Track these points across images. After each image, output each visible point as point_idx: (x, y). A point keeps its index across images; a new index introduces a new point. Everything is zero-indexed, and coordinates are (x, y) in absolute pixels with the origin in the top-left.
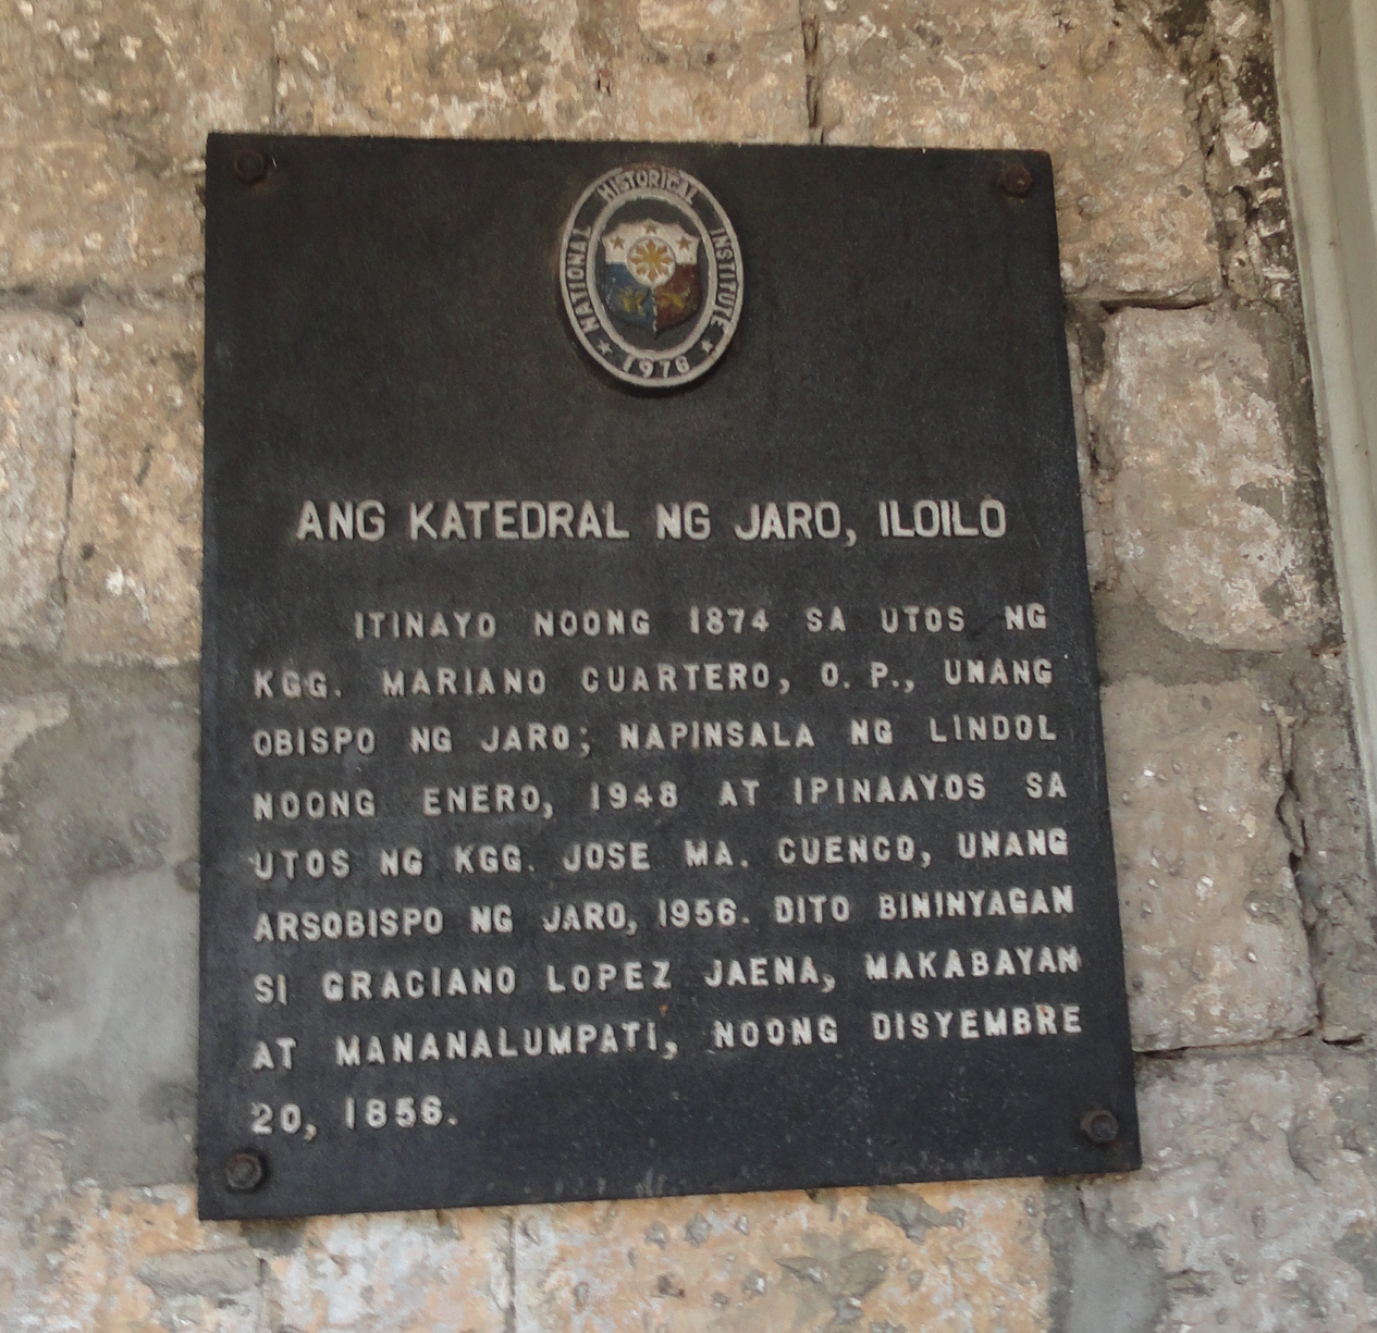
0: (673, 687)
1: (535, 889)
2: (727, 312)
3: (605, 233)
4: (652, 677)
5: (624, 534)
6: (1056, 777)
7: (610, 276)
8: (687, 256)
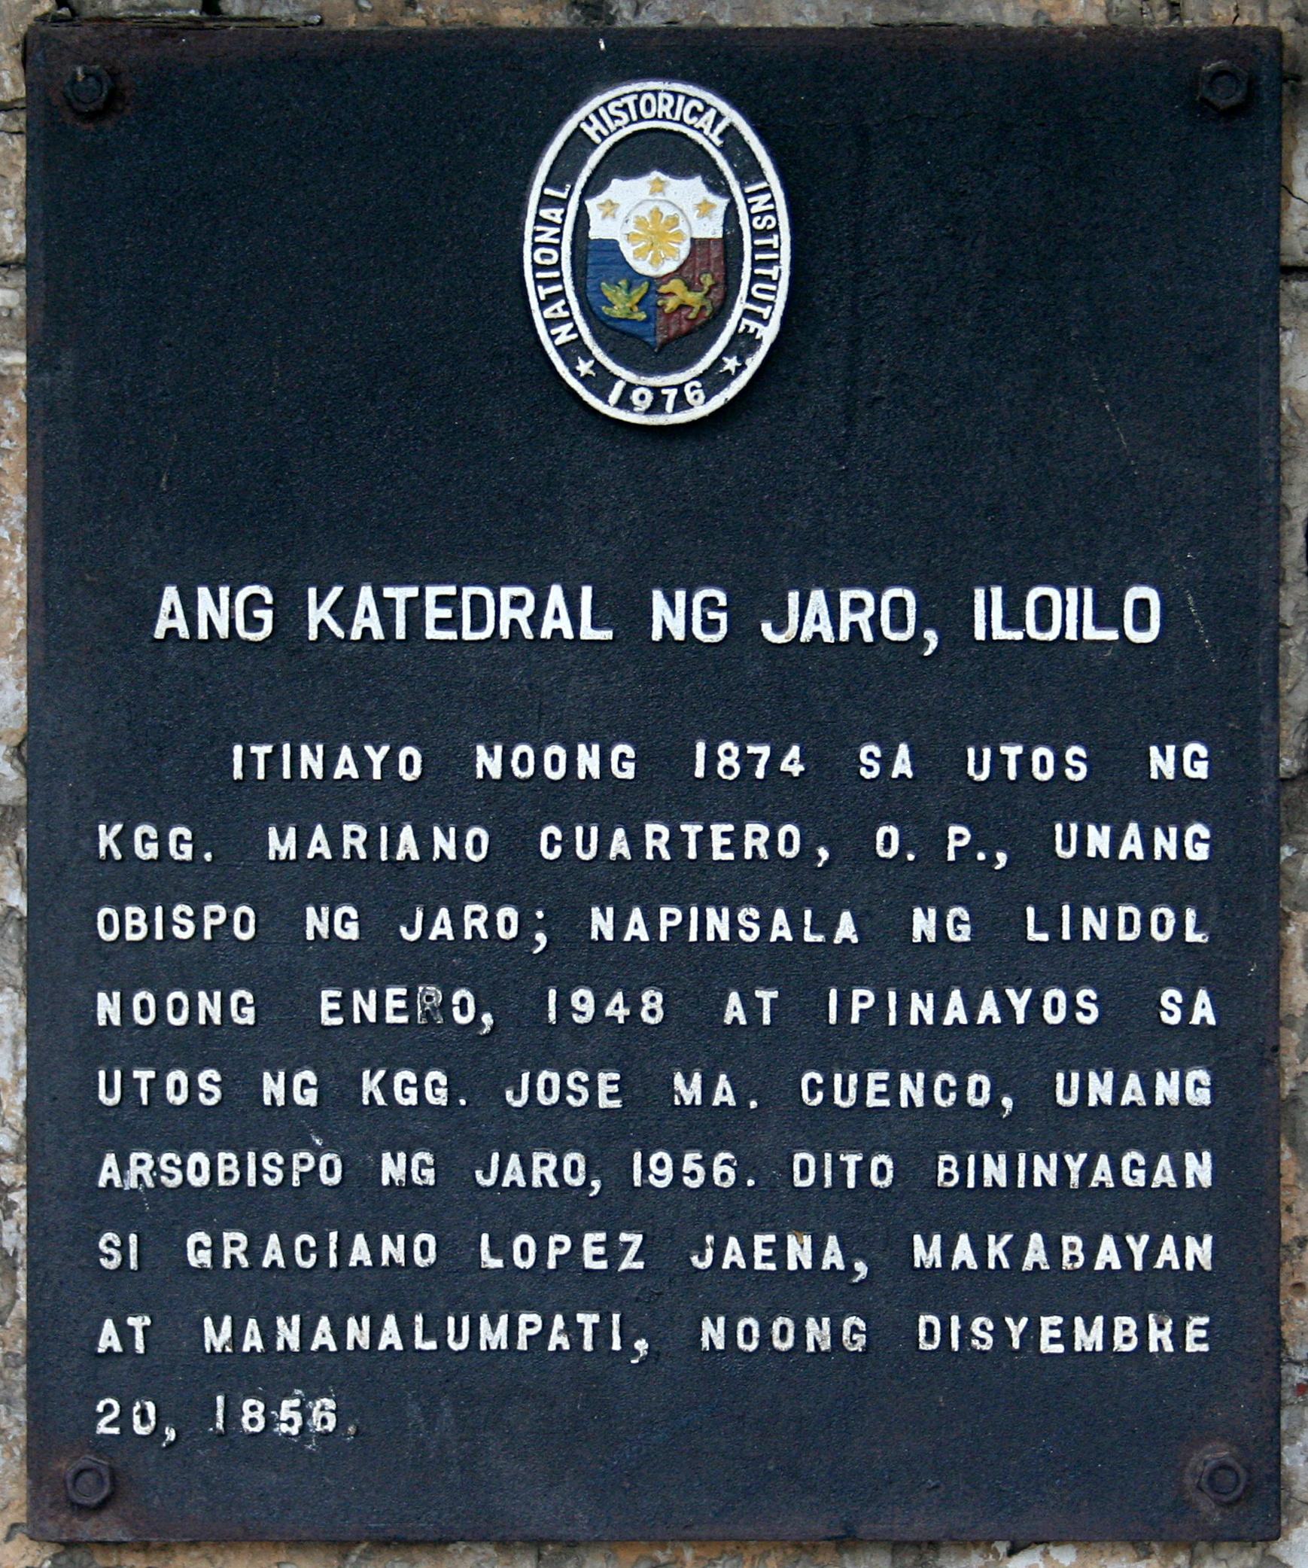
0: (666, 855)
1: (464, 1133)
2: (765, 312)
3: (586, 193)
4: (636, 840)
5: (607, 635)
6: (1203, 996)
7: (595, 260)
8: (712, 228)
